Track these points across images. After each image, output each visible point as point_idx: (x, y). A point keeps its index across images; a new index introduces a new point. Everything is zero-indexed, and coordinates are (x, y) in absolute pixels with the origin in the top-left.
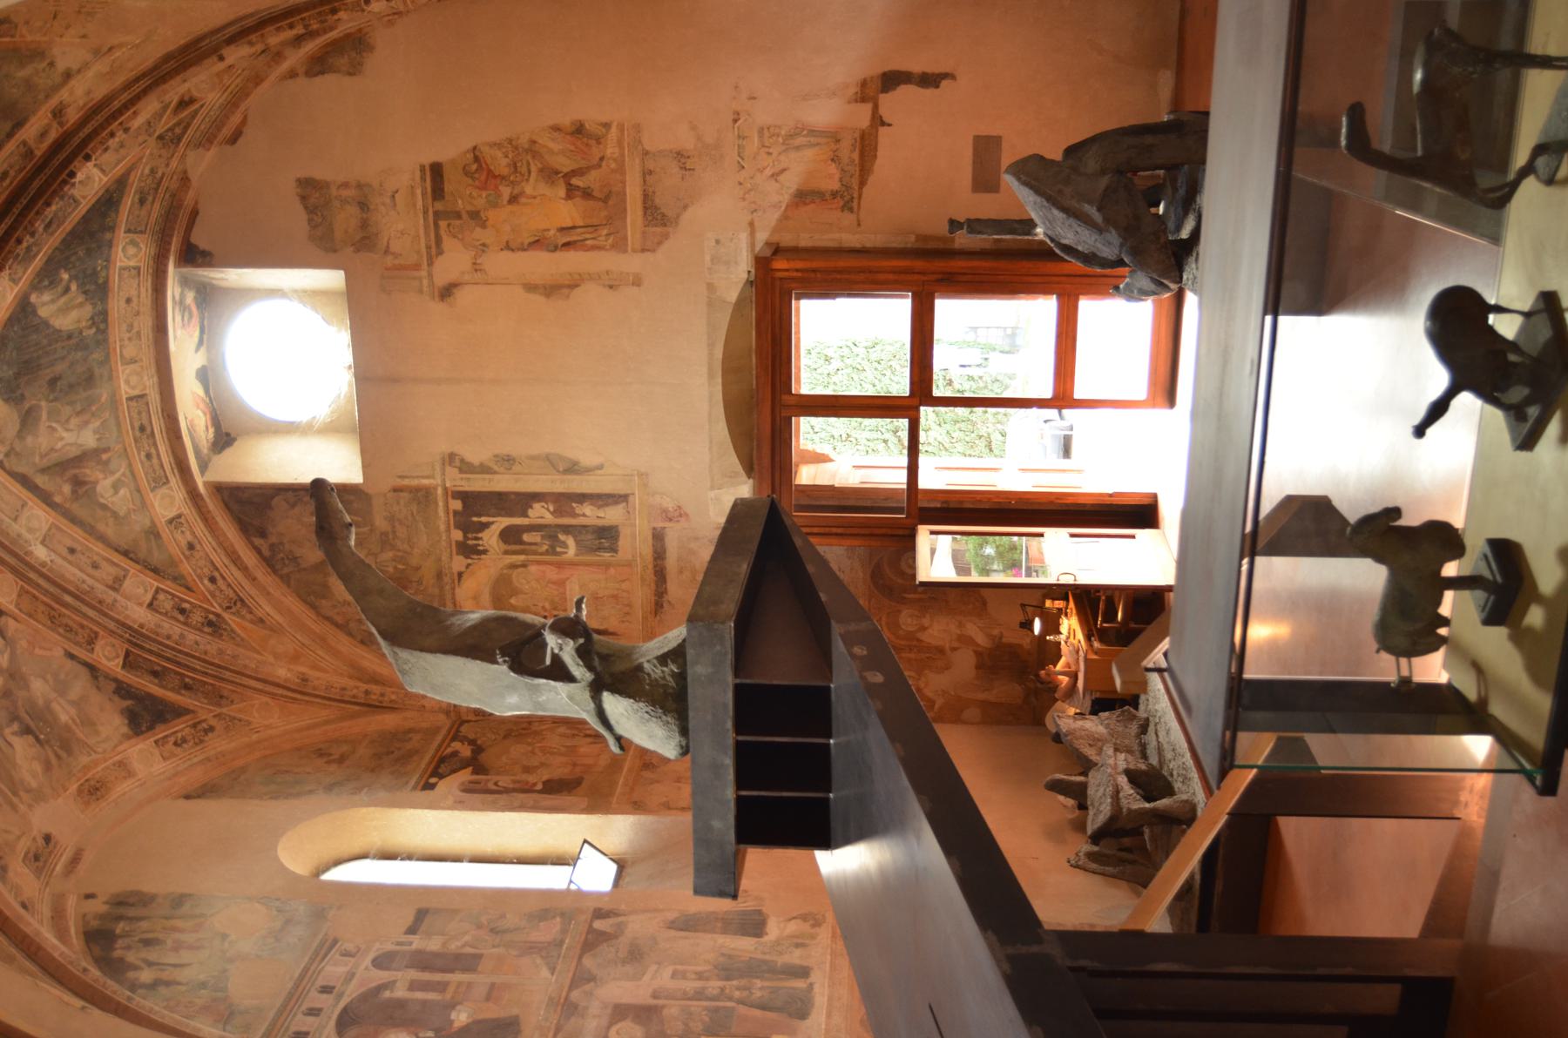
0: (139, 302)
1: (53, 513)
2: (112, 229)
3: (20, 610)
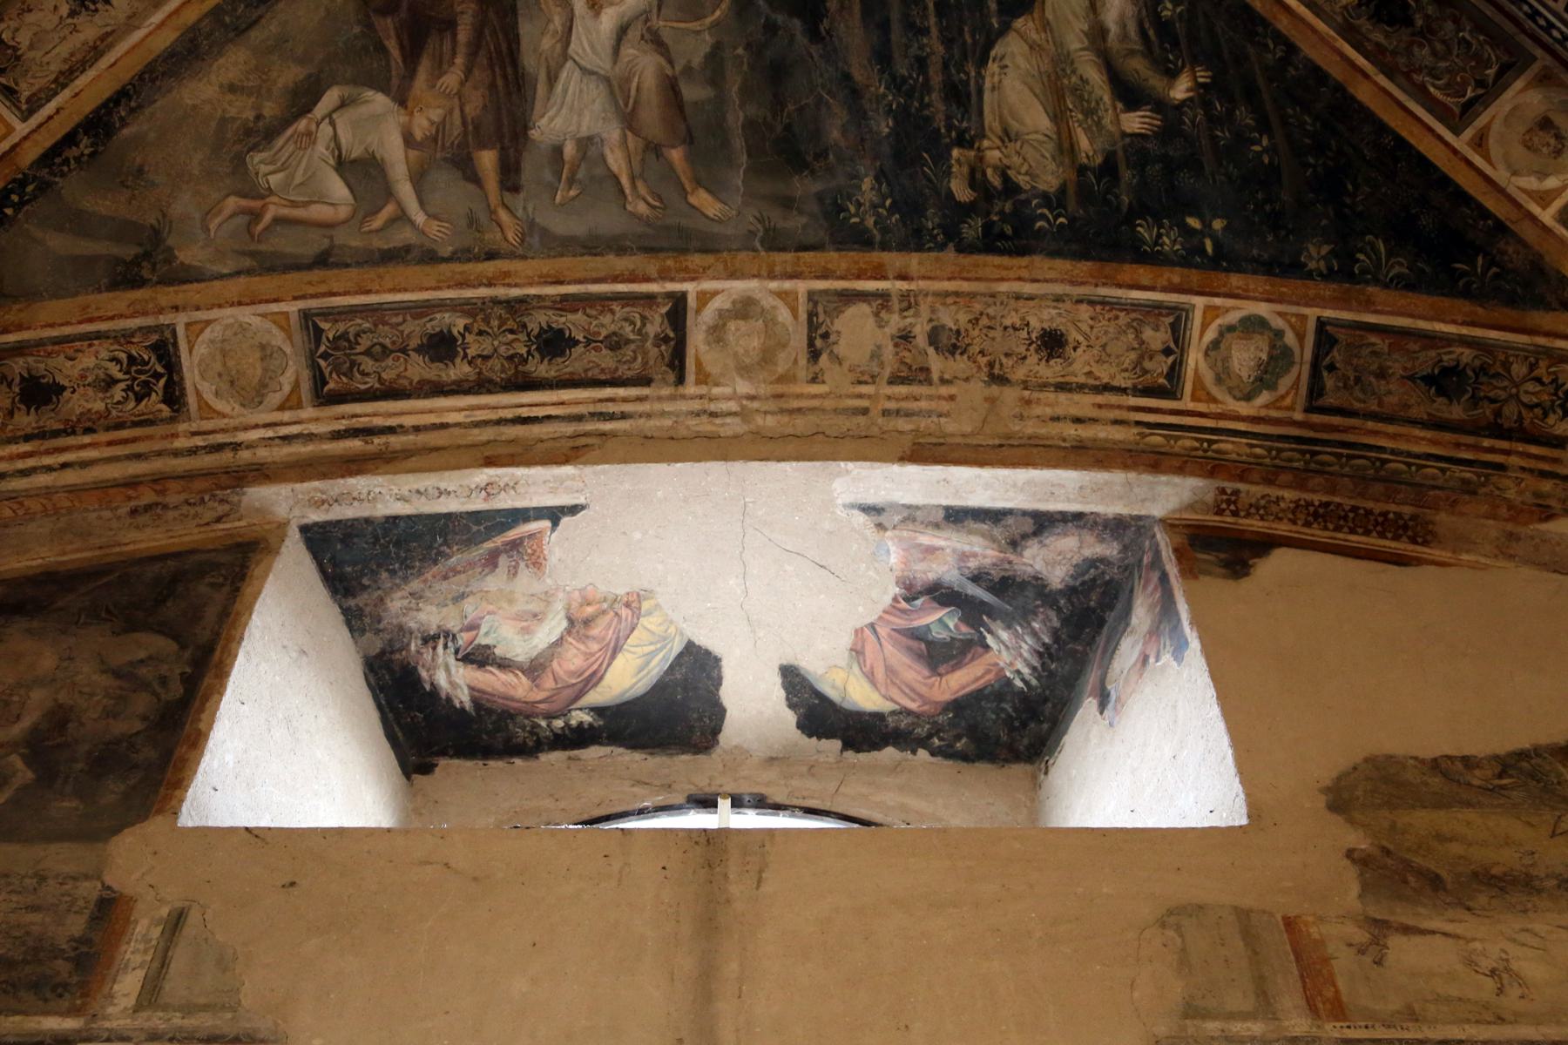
0: (1044, 386)
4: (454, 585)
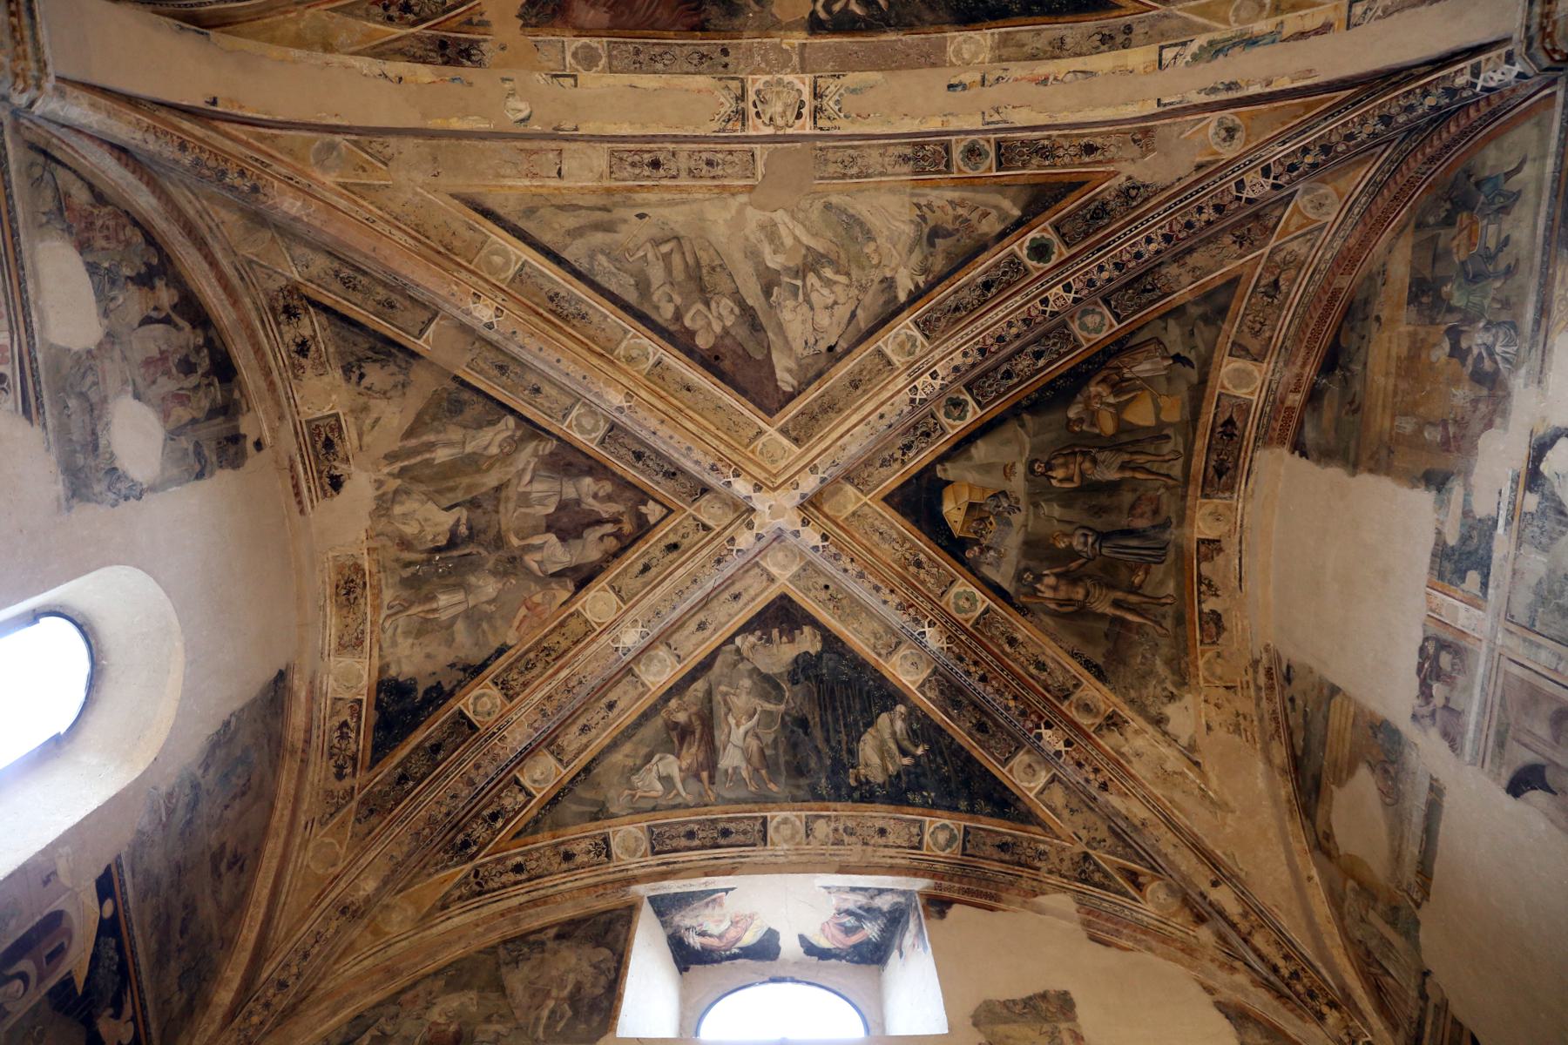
1: (660, 693)
2: (971, 810)
3: (572, 615)
4: (696, 913)
